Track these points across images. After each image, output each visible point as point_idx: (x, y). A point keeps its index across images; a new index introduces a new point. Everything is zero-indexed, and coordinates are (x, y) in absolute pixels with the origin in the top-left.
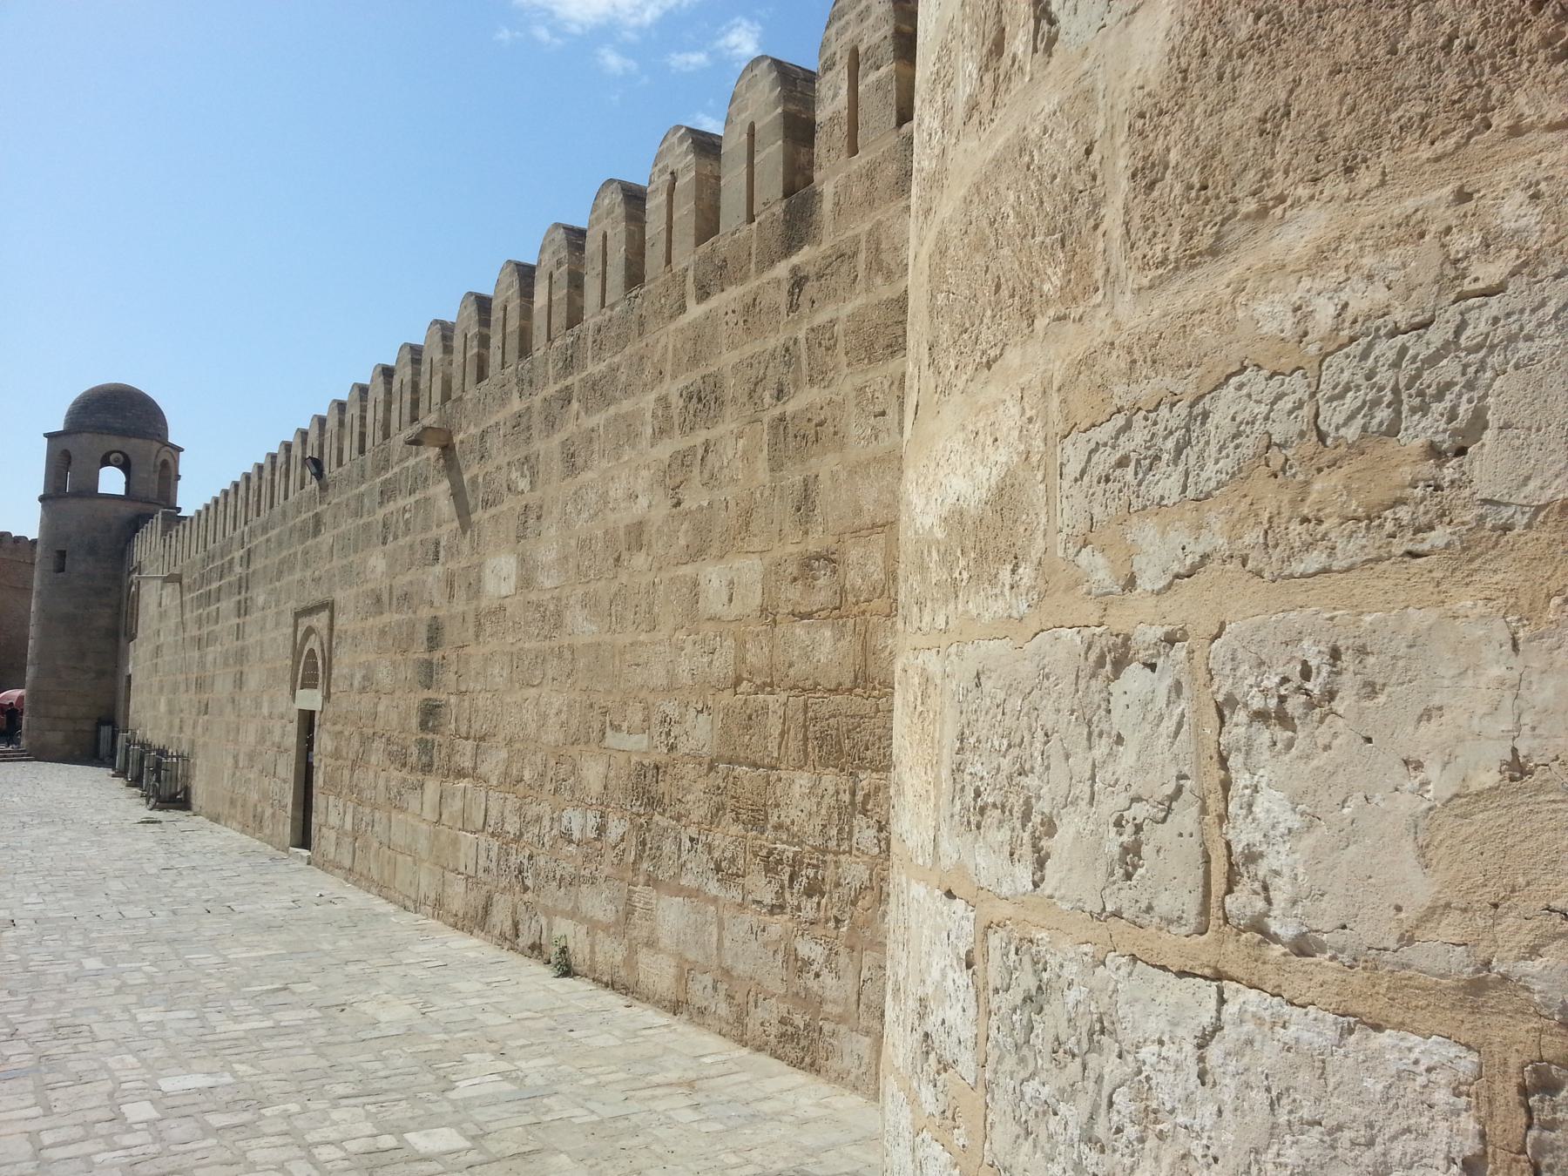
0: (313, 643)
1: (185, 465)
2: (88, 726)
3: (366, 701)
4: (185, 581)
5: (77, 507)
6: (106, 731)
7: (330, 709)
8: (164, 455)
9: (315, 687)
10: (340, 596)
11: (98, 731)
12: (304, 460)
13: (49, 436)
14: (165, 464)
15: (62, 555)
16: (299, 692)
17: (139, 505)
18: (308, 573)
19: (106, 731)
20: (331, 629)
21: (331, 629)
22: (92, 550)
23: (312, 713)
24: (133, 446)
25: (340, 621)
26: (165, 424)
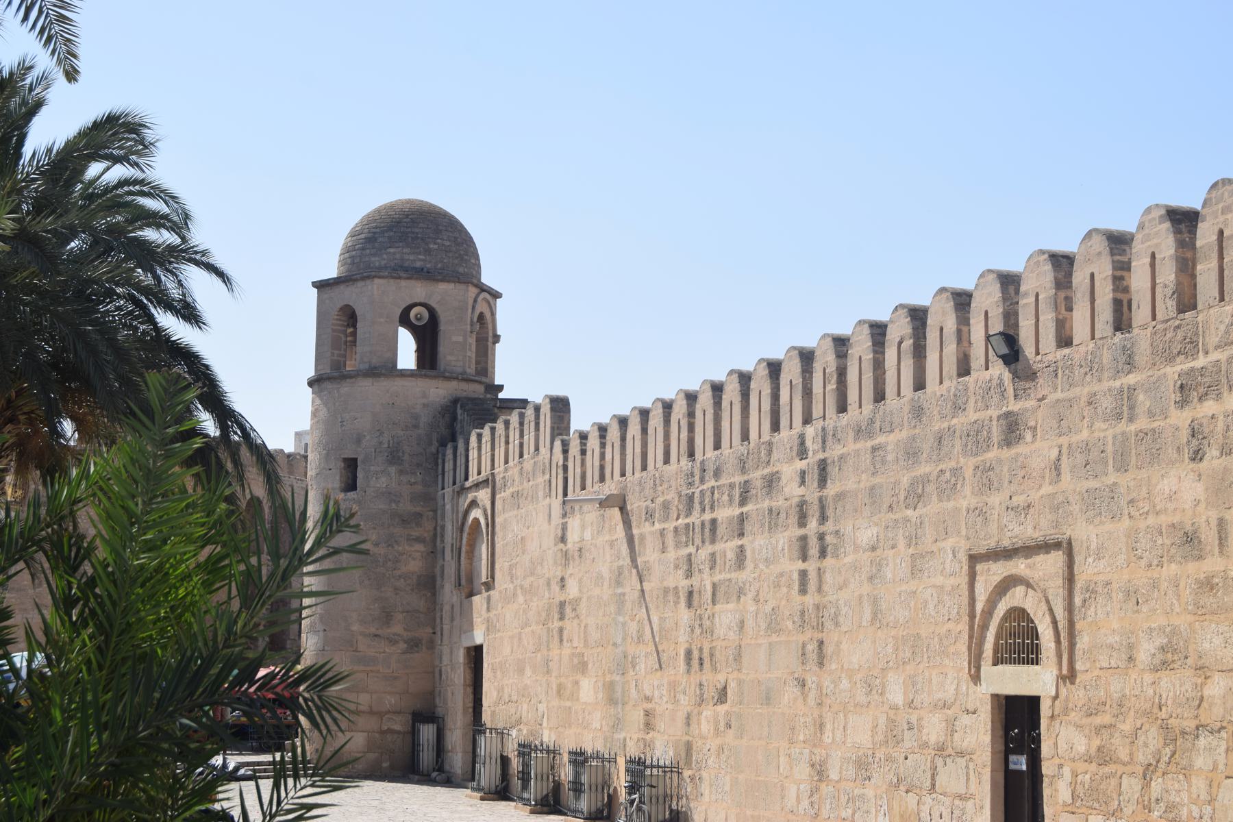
0: (1017, 597)
1: (505, 317)
2: (399, 724)
3: (1174, 685)
4: (634, 504)
5: (372, 392)
6: (427, 732)
7: (1076, 694)
8: (482, 307)
9: (1036, 662)
10: (1082, 532)
11: (414, 733)
12: (988, 337)
13: (321, 286)
14: (481, 317)
15: (351, 465)
16: (987, 668)
17: (454, 384)
18: (996, 499)
19: (427, 732)
20: (1070, 579)
21: (1070, 579)
22: (394, 457)
23: (1033, 703)
24: (441, 294)
25: (1087, 570)
26: (477, 258)
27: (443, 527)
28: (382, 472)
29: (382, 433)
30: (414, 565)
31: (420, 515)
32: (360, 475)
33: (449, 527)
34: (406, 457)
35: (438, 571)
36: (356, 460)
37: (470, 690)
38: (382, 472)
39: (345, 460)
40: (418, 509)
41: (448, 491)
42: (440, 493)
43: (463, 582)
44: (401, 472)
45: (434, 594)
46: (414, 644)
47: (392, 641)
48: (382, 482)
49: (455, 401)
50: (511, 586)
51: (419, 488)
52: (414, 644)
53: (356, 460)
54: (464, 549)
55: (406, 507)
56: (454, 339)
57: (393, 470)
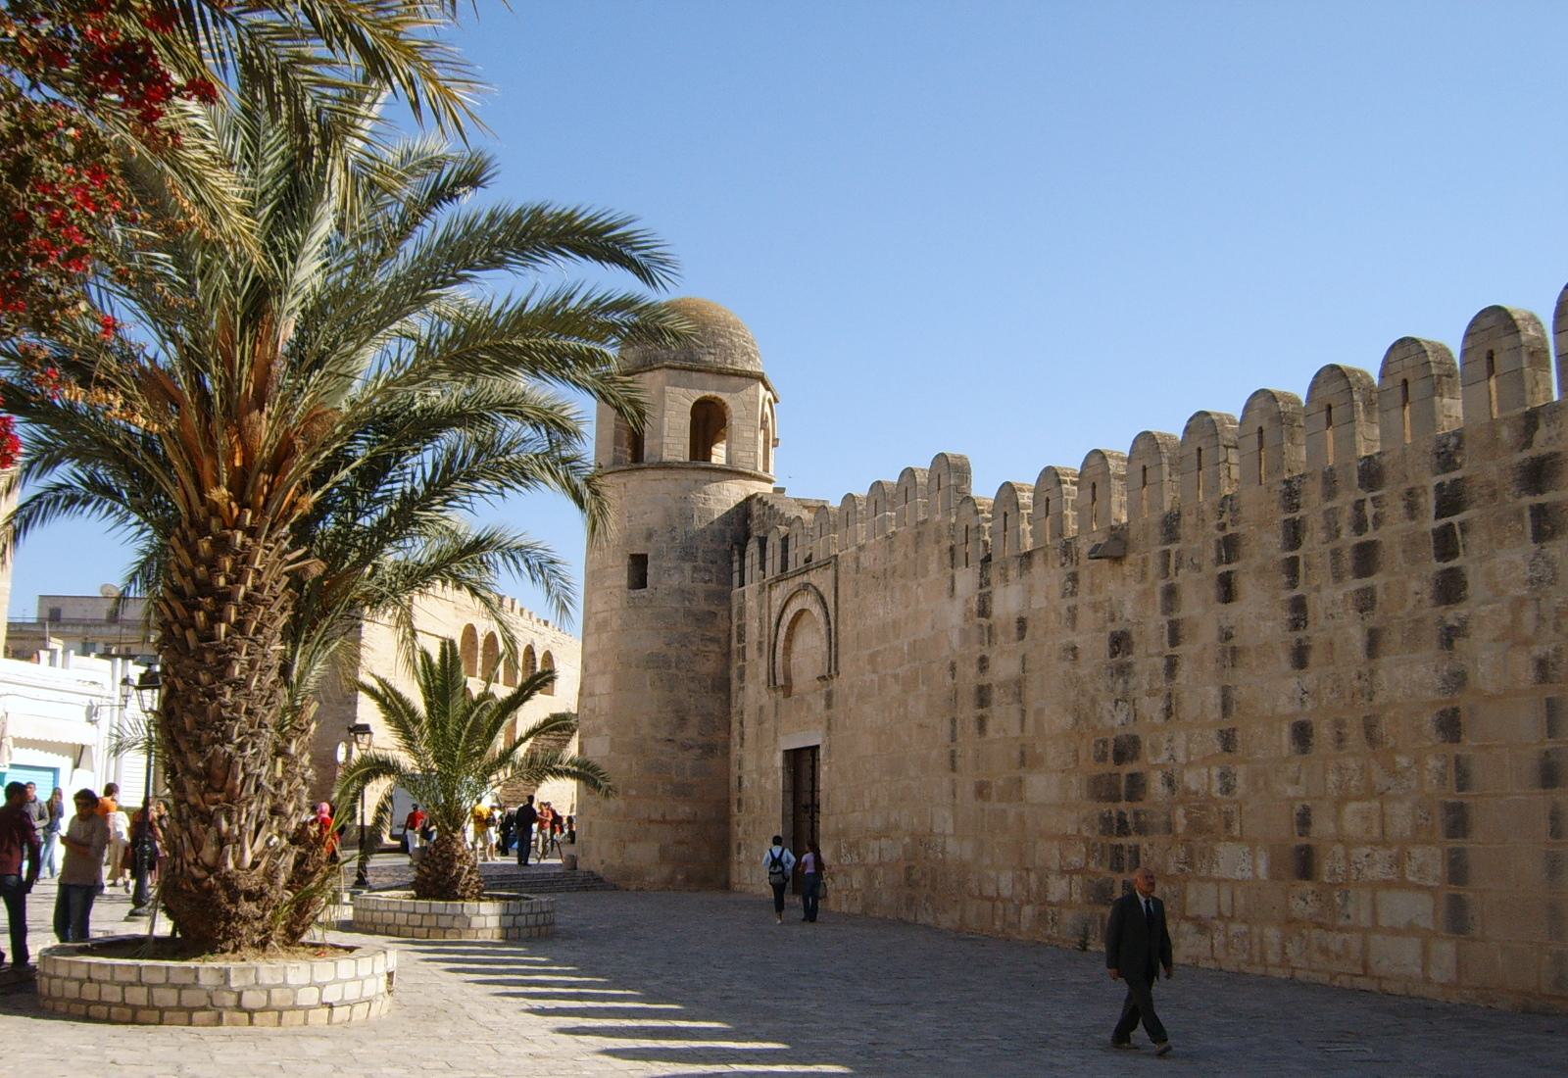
27: (741, 628)
28: (675, 568)
29: (674, 529)
30: (709, 666)
31: (716, 615)
32: (650, 571)
33: (753, 628)
34: (700, 553)
35: (734, 673)
36: (645, 556)
37: (790, 797)
38: (675, 568)
39: (633, 556)
40: (713, 608)
41: (751, 588)
42: (737, 591)
43: (780, 681)
44: (695, 569)
45: (729, 698)
46: (709, 750)
47: (685, 747)
48: (675, 580)
49: (749, 499)
50: (875, 677)
51: (713, 586)
52: (709, 750)
53: (645, 556)
54: (780, 644)
55: (701, 605)
56: (745, 435)
57: (687, 567)
